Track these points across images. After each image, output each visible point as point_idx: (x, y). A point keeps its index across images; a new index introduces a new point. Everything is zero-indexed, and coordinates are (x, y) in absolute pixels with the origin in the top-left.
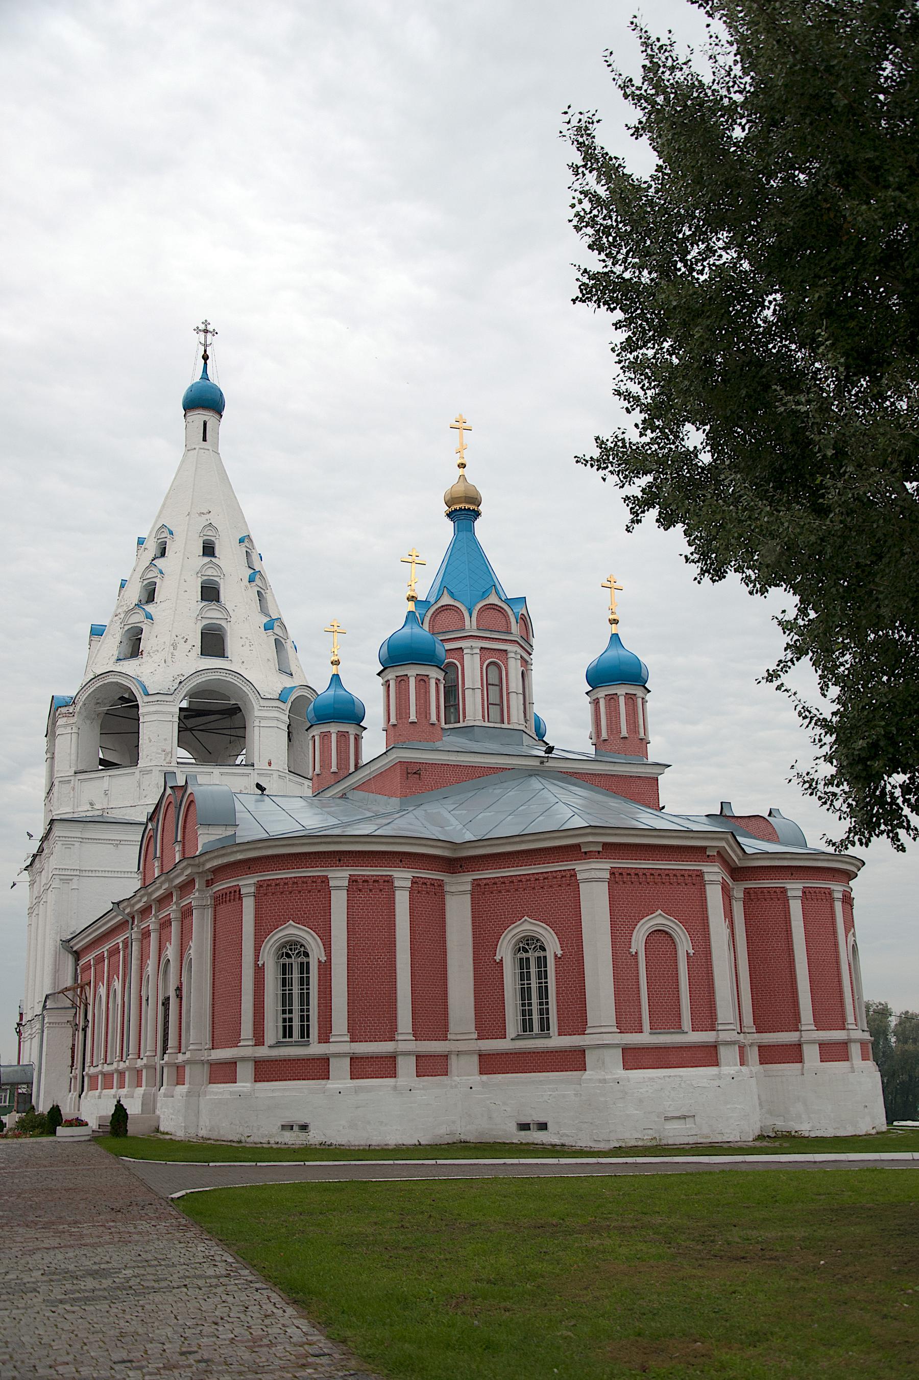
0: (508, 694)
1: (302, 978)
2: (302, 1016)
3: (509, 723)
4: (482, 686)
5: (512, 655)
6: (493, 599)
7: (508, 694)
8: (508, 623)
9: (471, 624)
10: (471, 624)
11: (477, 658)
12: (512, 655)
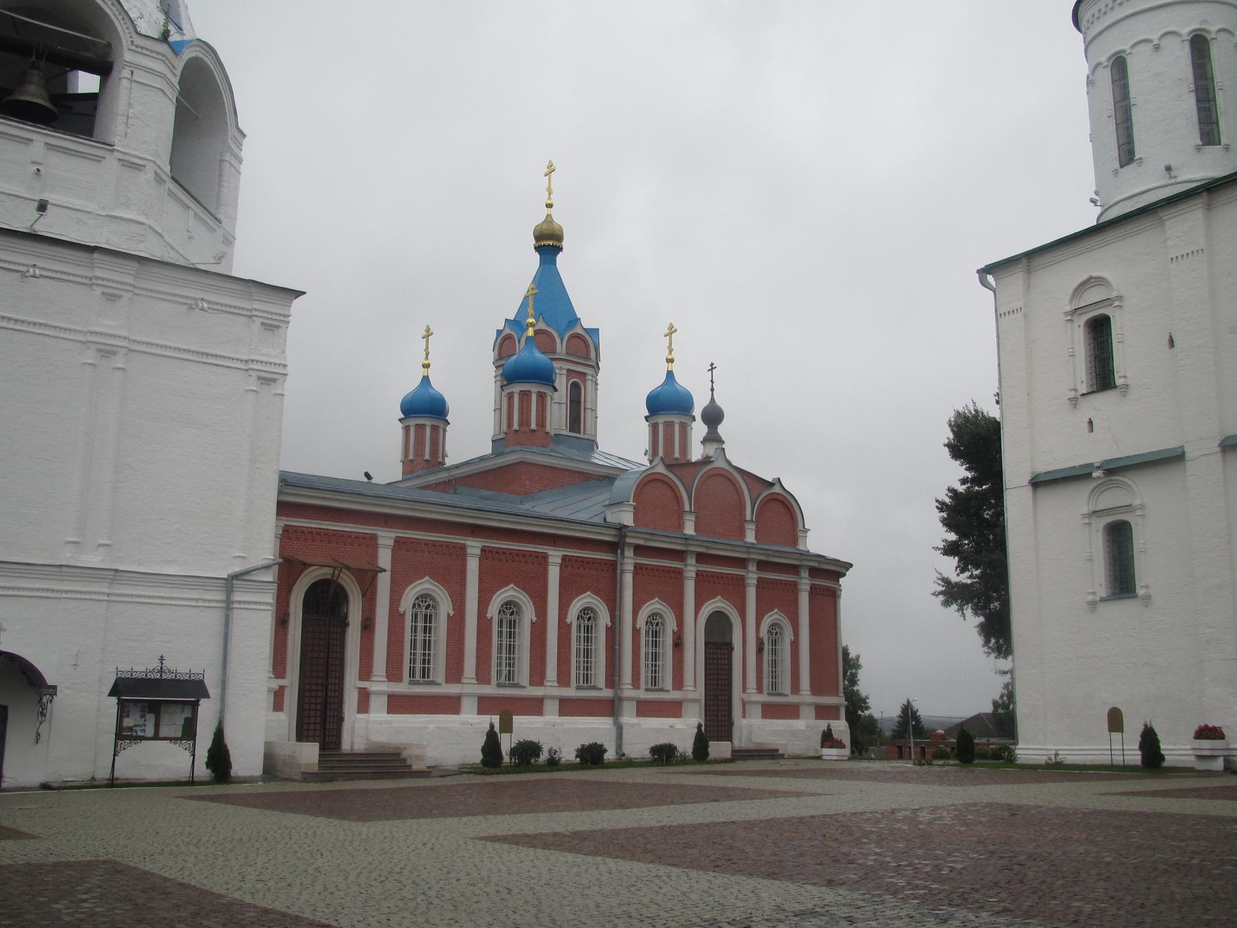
0: (585, 409)
1: (425, 627)
2: (424, 660)
3: (584, 434)
4: (567, 401)
5: (590, 377)
6: (578, 330)
7: (585, 409)
8: (588, 351)
9: (561, 348)
11: (564, 377)
12: (590, 377)
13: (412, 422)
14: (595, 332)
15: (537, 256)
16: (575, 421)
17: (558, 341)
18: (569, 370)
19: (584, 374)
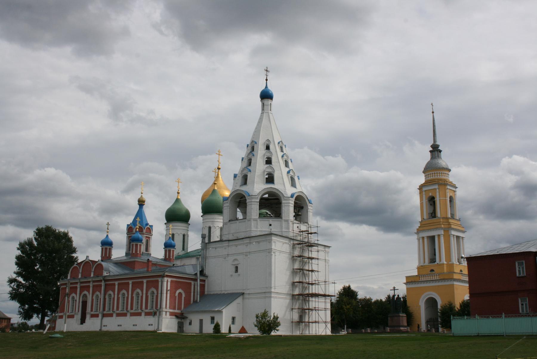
0: (149, 246)
6: (148, 226)
10: (145, 231)
11: (145, 238)
13: (104, 247)
14: (152, 226)
15: (138, 206)
16: (147, 249)
17: (144, 229)
18: (146, 237)
19: (149, 237)
